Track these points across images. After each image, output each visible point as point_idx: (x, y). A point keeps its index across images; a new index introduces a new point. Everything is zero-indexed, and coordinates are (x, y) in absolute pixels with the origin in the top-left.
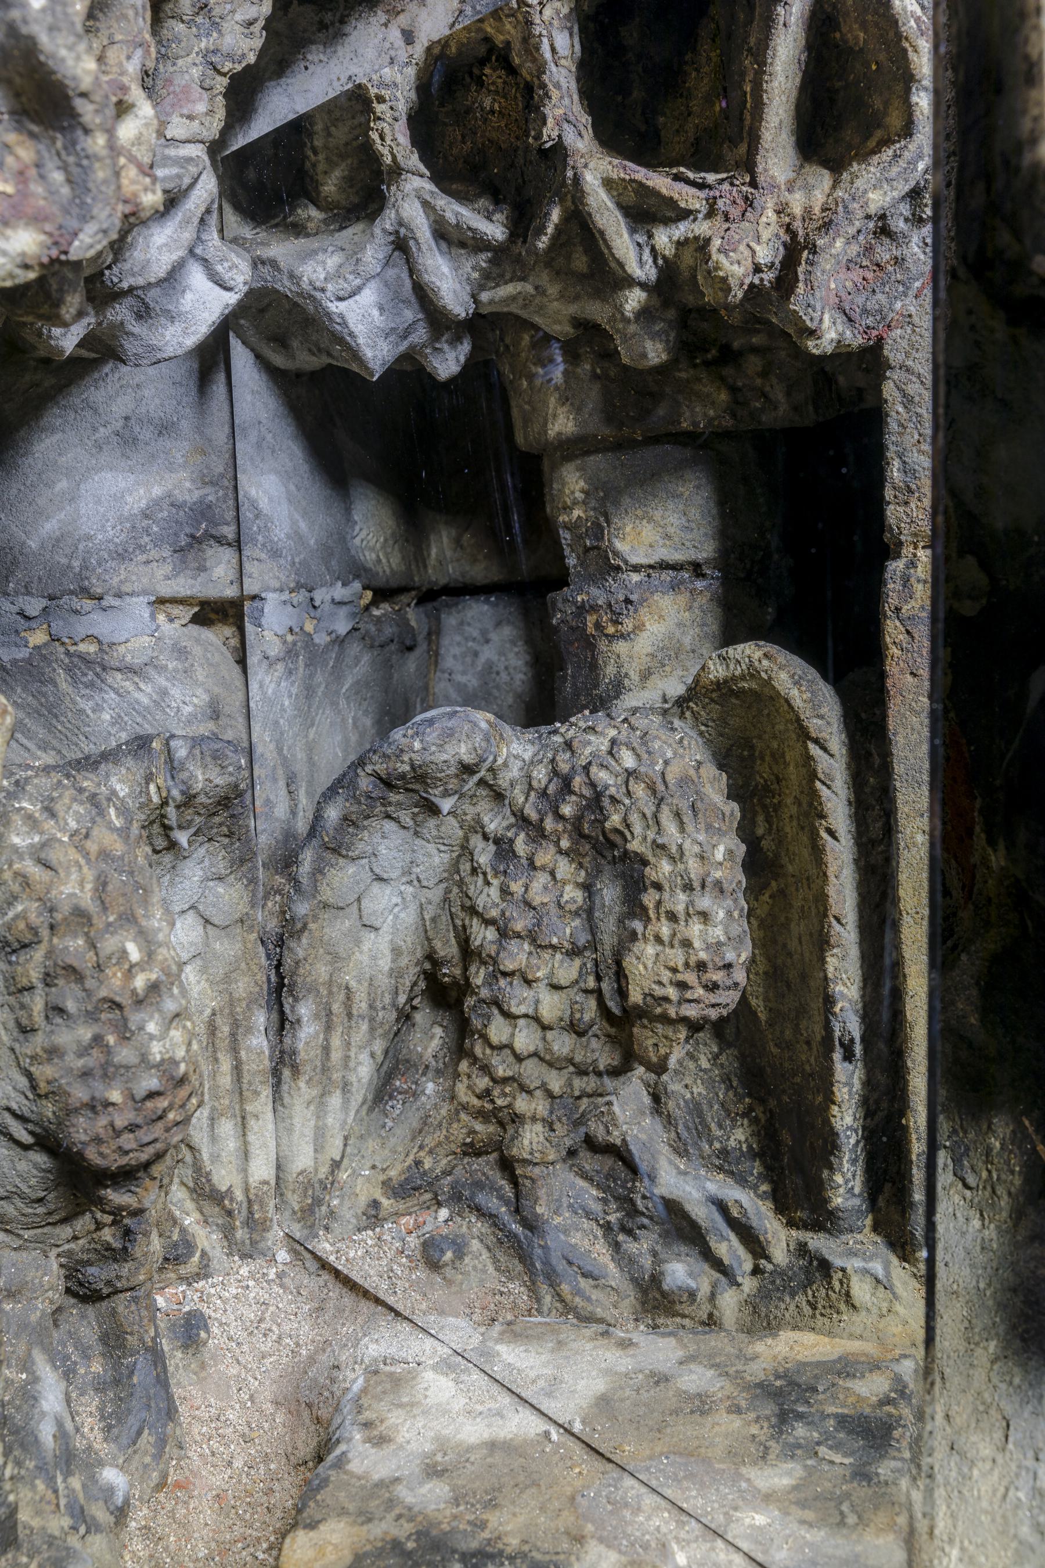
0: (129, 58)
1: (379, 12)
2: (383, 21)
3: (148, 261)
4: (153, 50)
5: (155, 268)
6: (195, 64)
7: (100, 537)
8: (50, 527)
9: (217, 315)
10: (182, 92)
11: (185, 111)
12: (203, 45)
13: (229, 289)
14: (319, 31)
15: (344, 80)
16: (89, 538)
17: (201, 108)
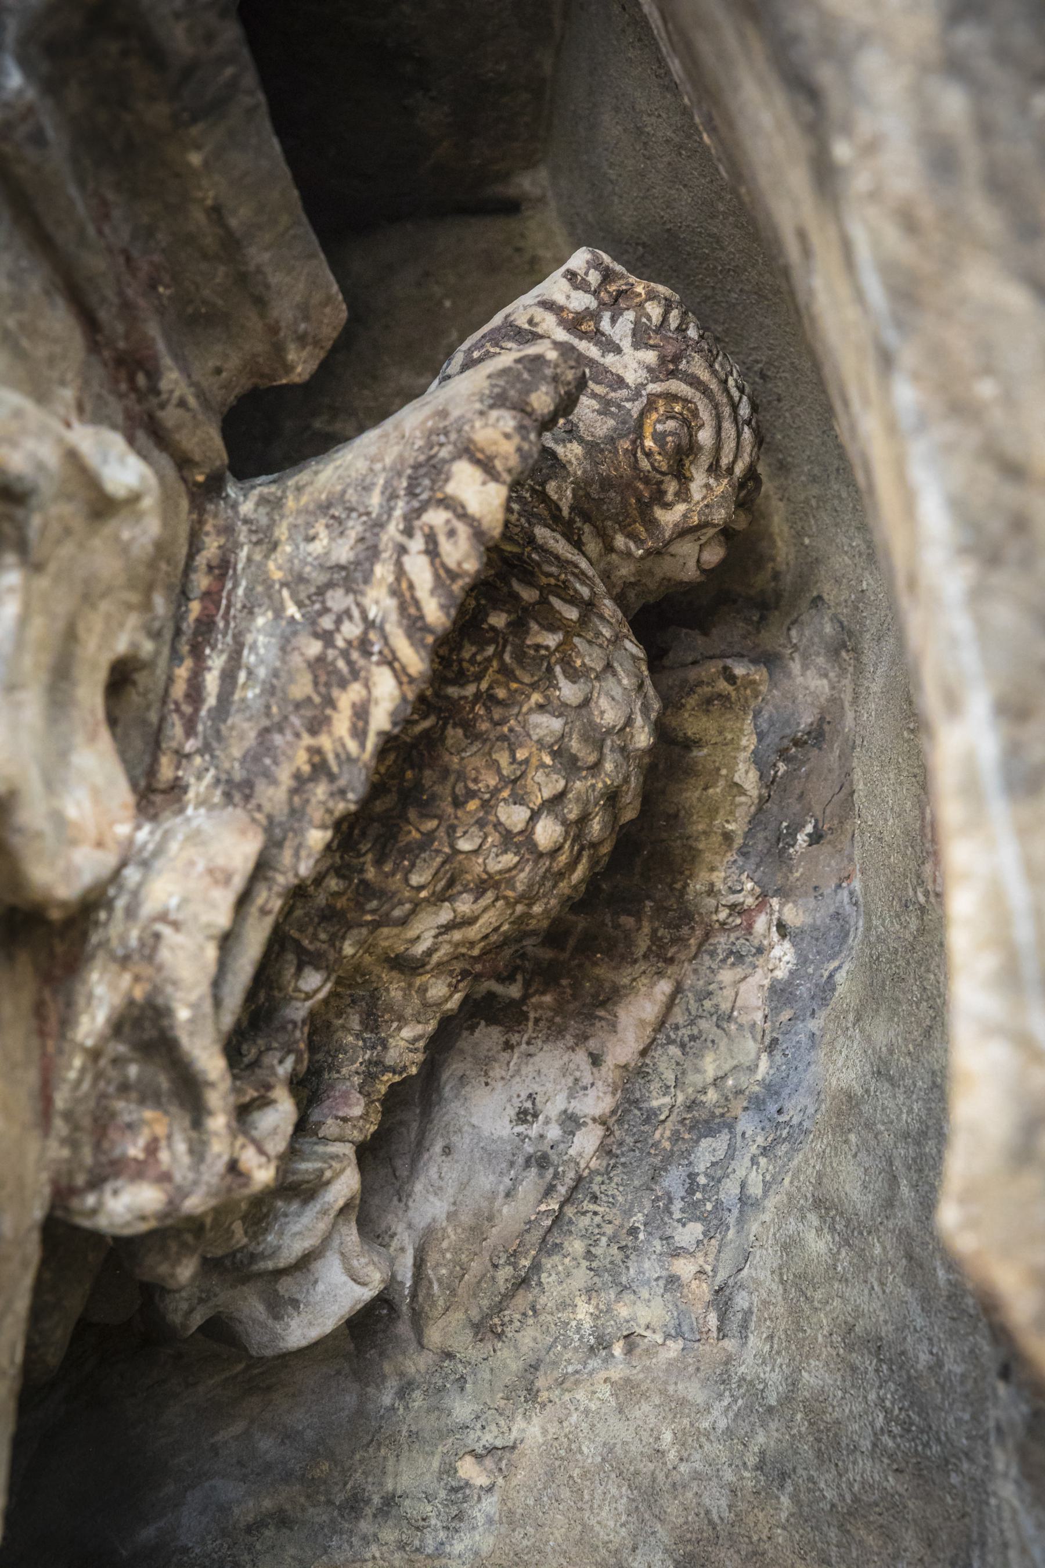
0: (281, 1062)
1: (568, 1037)
2: (571, 1043)
3: (279, 1247)
4: (306, 1056)
5: (285, 1253)
6: (357, 1073)
7: (197, 1551)
8: (148, 1534)
9: (347, 1309)
10: (341, 1096)
11: (341, 1114)
12: (367, 1057)
13: (364, 1284)
14: (504, 1050)
15: (524, 1095)
16: (185, 1550)
17: (357, 1111)
